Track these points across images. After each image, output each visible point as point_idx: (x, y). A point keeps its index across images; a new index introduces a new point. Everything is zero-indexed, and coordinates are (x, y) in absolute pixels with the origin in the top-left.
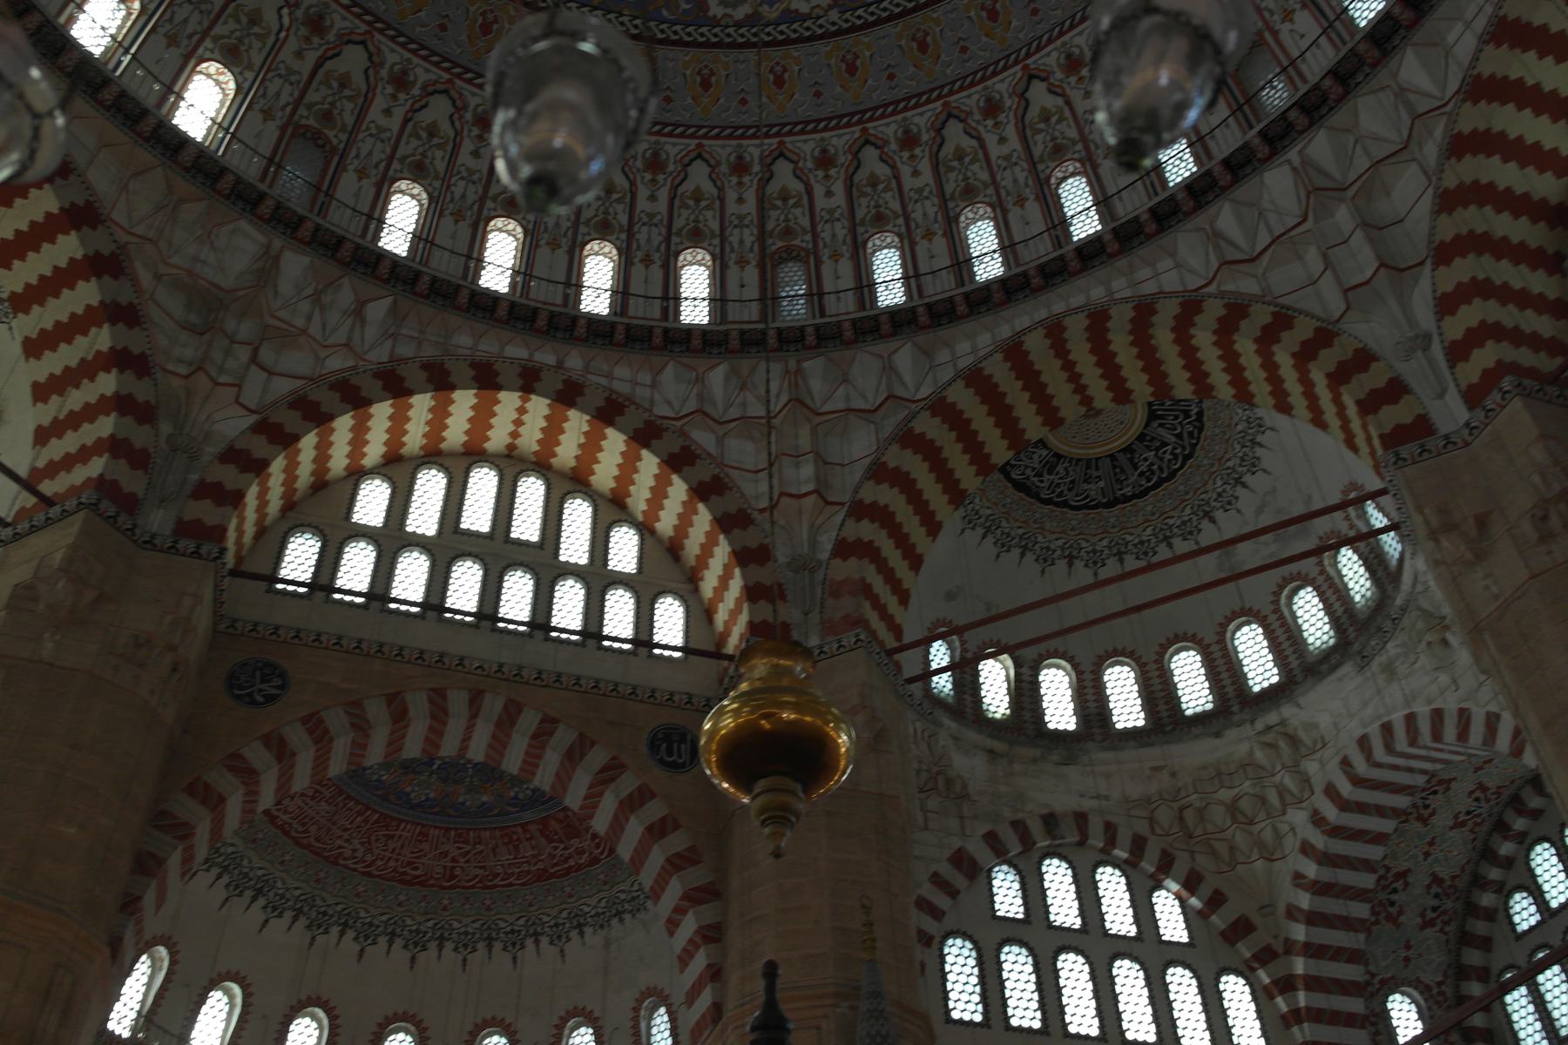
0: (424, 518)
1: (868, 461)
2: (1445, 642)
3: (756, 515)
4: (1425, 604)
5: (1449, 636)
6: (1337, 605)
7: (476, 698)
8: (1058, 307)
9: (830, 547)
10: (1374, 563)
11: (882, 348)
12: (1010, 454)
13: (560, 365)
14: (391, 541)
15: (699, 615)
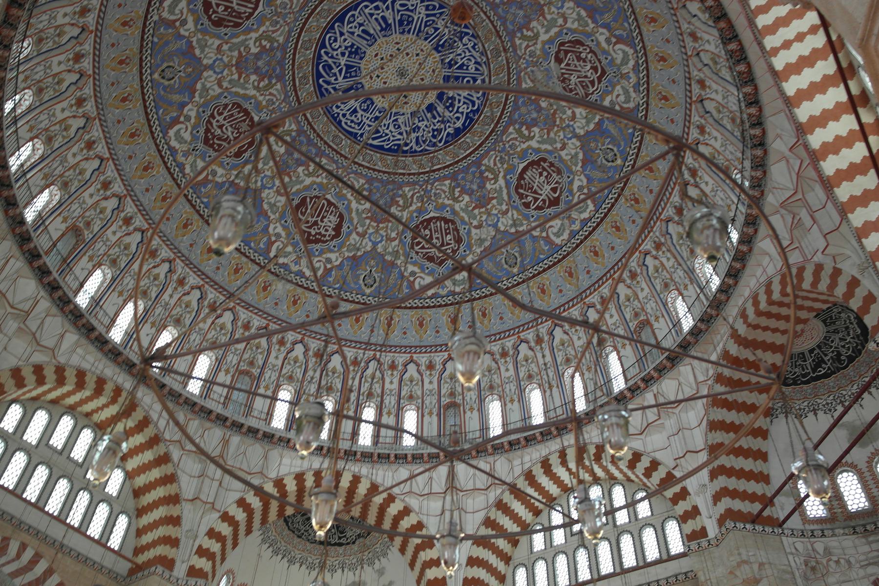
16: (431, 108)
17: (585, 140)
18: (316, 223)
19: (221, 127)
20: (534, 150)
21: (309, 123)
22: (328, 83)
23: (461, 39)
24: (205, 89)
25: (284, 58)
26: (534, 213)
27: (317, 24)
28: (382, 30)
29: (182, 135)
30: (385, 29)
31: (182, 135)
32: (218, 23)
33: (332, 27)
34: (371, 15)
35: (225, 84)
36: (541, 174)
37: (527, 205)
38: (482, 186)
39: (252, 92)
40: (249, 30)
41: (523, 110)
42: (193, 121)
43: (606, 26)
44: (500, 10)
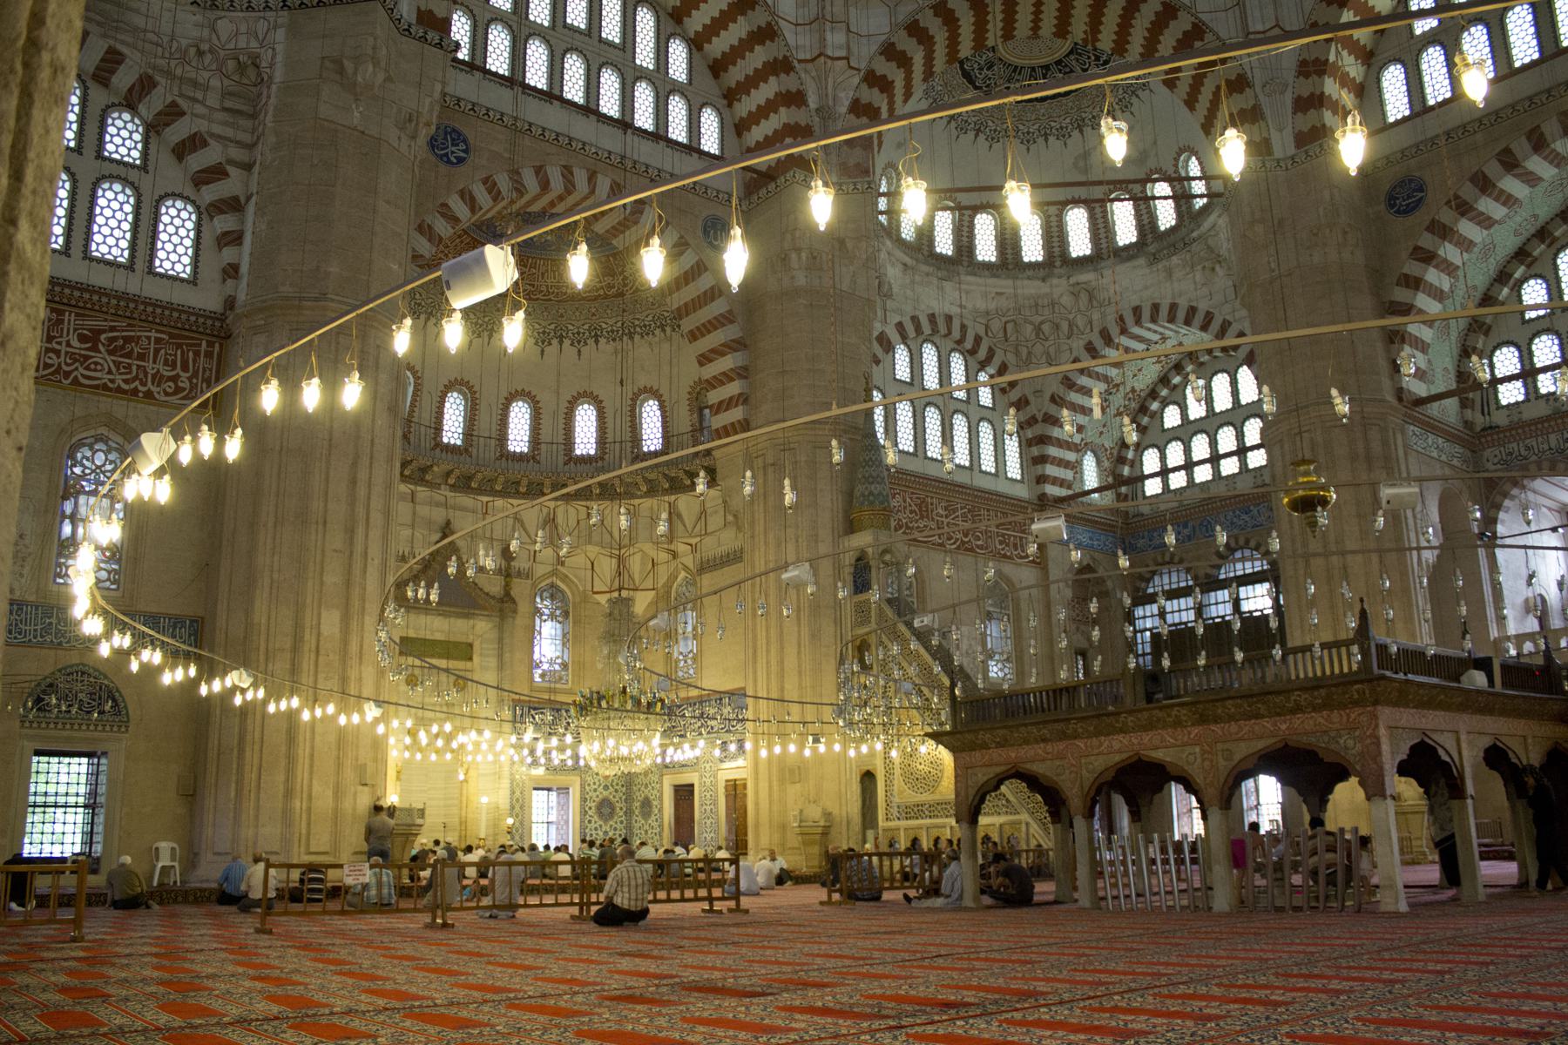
1: (884, 38)
2: (1213, 269)
3: (795, 63)
4: (1210, 242)
5: (1218, 268)
6: (1145, 217)
7: (592, 178)
9: (847, 103)
10: (1182, 198)
15: (734, 129)
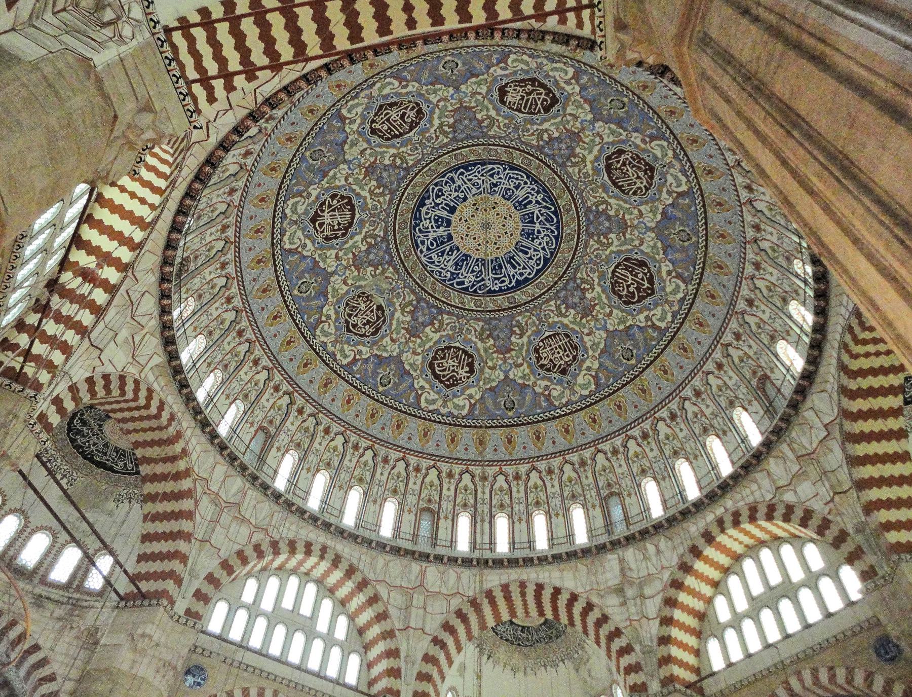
0: (742, 605)
3: (830, 517)
8: (838, 337)
11: (808, 403)
12: (901, 397)
13: (726, 510)
14: (736, 623)
16: (452, 210)
17: (327, 276)
18: (529, 94)
19: (638, 177)
20: (356, 234)
21: (556, 173)
22: (545, 207)
23: (452, 274)
24: (653, 211)
25: (588, 226)
26: (323, 198)
27: (565, 255)
28: (512, 258)
29: (675, 180)
30: (512, 258)
31: (675, 180)
32: (642, 264)
33: (552, 253)
34: (524, 268)
35: (636, 212)
36: (339, 224)
37: (333, 197)
38: (379, 179)
39: (612, 201)
40: (619, 253)
41: (381, 253)
42: (665, 190)
43: (366, 361)
44: (435, 311)
